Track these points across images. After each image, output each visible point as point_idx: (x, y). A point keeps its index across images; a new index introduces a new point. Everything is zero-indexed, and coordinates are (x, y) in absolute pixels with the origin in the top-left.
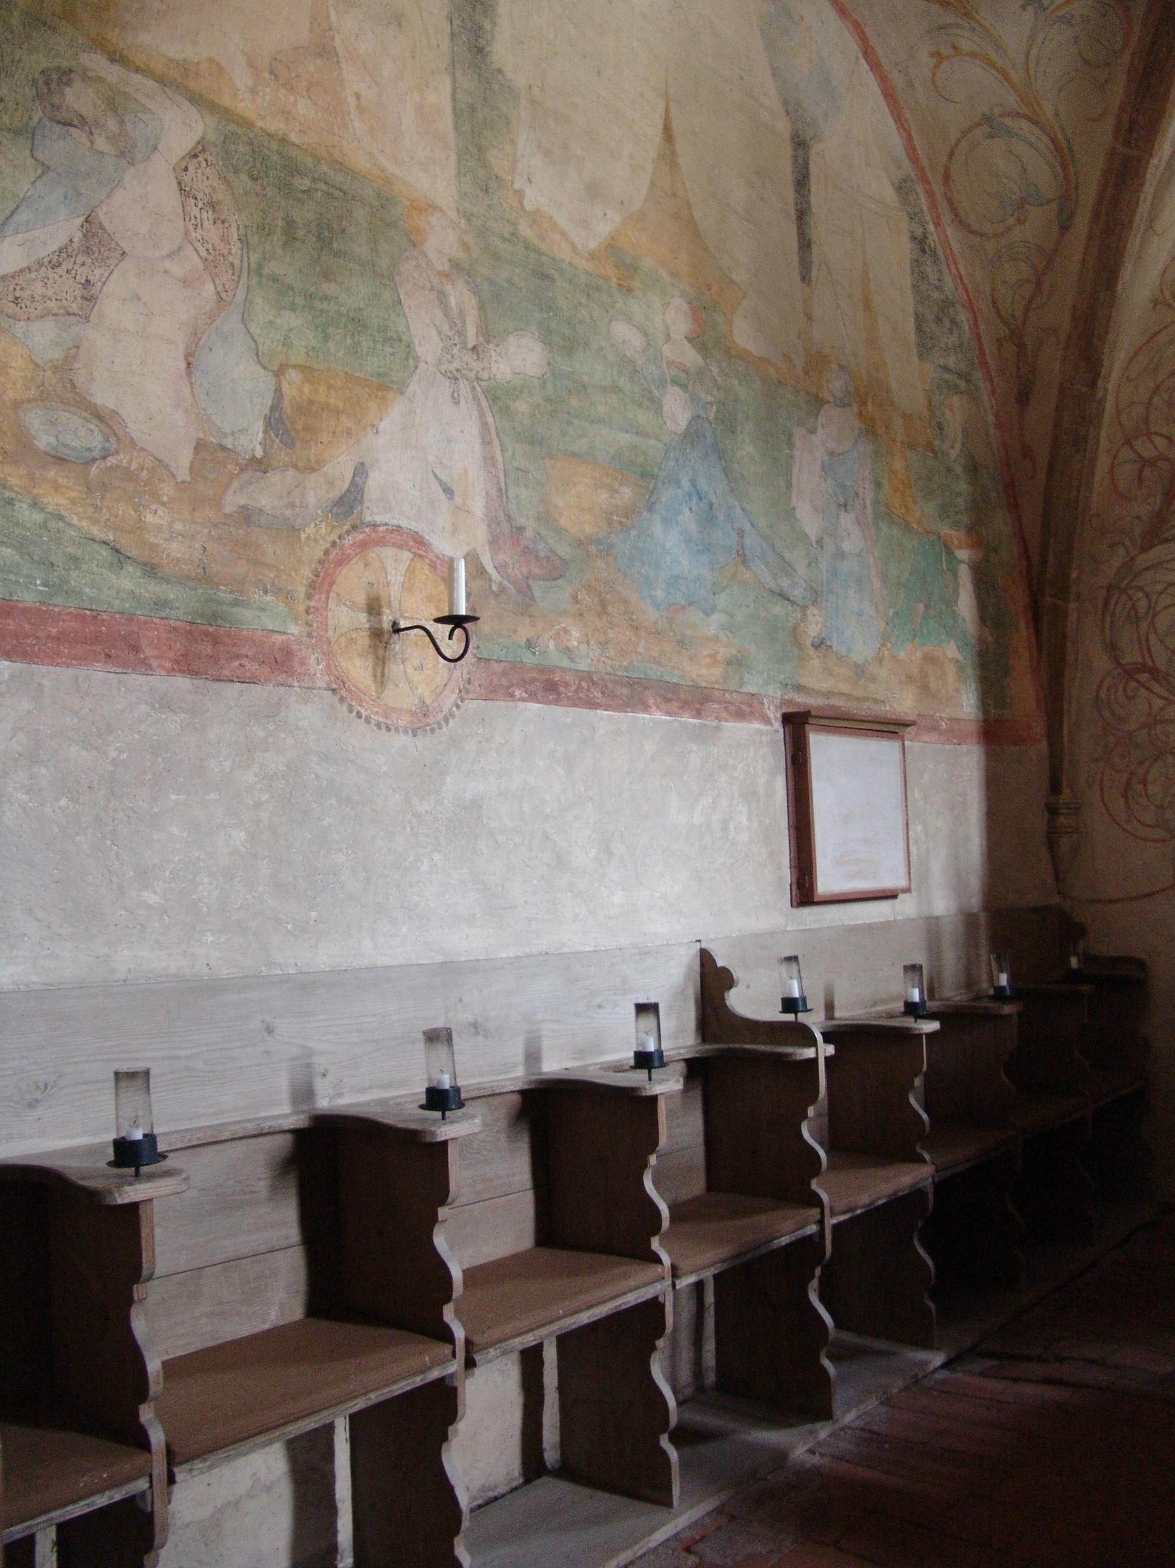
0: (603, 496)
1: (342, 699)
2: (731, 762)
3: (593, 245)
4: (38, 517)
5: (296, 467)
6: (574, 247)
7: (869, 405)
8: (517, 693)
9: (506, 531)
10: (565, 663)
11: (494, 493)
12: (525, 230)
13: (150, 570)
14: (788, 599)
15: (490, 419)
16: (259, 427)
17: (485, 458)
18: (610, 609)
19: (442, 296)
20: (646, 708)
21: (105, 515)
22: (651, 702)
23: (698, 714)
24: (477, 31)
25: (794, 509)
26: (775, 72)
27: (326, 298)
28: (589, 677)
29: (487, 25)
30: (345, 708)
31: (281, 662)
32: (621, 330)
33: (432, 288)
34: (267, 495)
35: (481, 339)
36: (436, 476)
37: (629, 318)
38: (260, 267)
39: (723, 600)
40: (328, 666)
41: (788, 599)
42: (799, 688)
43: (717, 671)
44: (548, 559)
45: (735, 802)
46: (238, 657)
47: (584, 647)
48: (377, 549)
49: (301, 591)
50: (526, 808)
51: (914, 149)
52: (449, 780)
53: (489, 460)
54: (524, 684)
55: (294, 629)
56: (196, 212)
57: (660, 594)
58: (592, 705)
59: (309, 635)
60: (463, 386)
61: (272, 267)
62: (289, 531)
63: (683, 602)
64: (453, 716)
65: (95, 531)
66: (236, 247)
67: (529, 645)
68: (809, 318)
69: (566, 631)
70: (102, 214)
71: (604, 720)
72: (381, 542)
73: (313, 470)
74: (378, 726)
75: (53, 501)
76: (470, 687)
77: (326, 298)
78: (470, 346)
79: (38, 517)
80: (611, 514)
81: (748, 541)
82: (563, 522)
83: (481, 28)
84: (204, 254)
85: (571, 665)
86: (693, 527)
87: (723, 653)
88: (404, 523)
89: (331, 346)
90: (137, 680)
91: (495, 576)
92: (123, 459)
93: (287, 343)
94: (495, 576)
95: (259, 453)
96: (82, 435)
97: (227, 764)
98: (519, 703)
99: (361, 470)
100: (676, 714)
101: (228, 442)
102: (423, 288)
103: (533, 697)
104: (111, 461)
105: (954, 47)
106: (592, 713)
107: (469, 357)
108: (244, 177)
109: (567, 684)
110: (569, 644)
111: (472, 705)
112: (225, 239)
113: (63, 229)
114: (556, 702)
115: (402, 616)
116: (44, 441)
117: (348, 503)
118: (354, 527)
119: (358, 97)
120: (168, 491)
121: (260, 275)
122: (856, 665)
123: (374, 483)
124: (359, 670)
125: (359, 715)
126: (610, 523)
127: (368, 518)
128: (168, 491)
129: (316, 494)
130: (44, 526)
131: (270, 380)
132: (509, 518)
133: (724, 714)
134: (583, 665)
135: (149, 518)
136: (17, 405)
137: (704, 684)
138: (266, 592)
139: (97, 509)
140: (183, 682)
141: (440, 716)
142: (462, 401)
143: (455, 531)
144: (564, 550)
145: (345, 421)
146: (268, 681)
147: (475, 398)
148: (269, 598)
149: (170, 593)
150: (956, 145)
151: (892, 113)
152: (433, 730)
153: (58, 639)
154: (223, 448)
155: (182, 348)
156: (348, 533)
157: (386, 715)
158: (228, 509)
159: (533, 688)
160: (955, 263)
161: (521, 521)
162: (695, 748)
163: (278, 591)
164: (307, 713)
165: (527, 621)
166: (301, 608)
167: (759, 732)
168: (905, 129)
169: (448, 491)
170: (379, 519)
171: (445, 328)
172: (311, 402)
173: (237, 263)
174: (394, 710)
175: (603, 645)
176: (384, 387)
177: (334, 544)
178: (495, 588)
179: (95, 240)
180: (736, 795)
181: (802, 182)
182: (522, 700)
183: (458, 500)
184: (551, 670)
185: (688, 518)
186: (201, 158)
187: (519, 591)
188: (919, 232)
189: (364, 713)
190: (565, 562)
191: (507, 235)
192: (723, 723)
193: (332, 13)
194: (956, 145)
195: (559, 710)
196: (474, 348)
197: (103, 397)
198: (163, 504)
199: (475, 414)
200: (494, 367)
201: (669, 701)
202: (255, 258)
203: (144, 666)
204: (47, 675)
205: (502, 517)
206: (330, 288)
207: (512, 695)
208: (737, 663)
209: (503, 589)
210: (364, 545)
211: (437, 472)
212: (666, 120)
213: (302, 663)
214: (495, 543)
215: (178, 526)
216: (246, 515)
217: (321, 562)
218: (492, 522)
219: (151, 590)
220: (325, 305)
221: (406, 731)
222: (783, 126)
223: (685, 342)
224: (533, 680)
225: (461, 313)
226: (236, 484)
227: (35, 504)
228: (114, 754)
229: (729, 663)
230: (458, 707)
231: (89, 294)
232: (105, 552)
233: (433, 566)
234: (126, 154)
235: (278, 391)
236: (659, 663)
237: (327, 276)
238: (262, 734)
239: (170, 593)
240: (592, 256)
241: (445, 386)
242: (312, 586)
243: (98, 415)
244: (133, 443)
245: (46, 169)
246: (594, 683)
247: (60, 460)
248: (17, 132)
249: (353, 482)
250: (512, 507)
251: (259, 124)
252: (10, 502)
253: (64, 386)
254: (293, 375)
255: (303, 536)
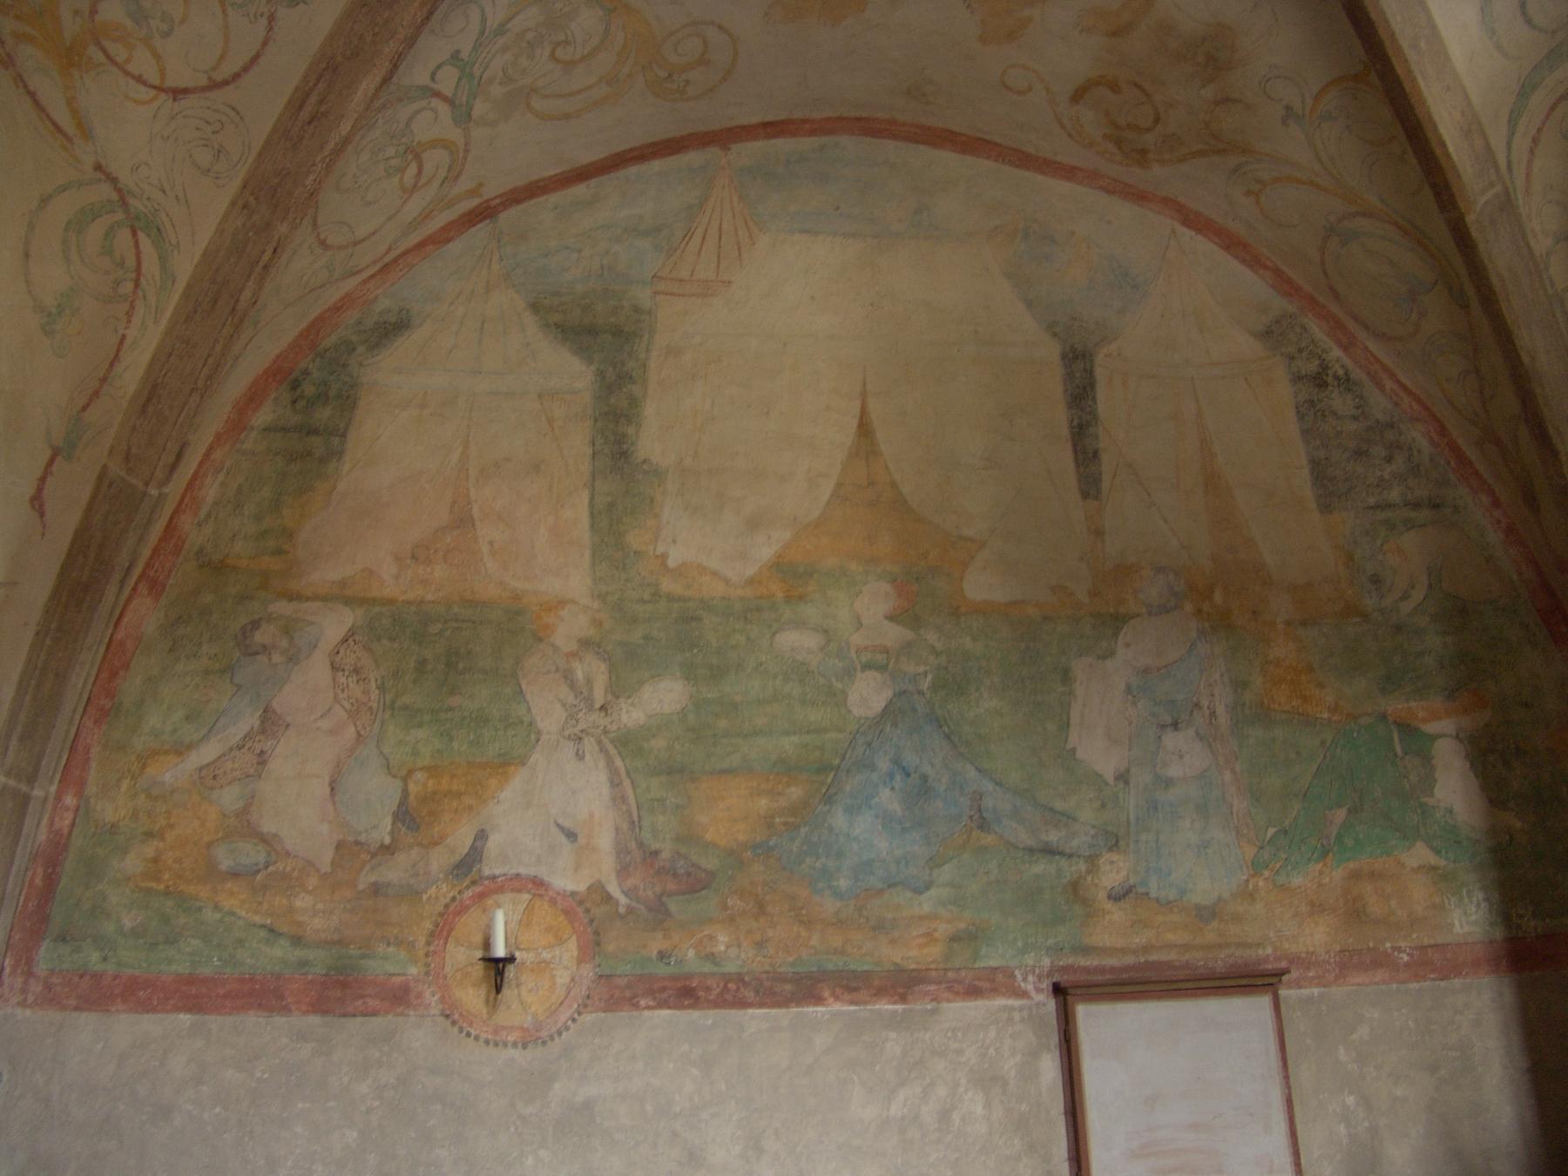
0: (763, 803)
1: (454, 1023)
2: (954, 1045)
3: (750, 571)
4: (218, 916)
5: (420, 844)
6: (727, 581)
7: (1219, 600)
8: (643, 1003)
9: (637, 855)
10: (708, 968)
11: (625, 826)
12: (667, 585)
13: (297, 941)
14: (1061, 854)
15: (619, 762)
16: (389, 820)
17: (614, 799)
18: (769, 908)
19: (568, 677)
20: (819, 1000)
21: (265, 906)
22: (826, 994)
23: (903, 999)
24: (621, 439)
25: (1074, 750)
26: (1029, 304)
27: (451, 709)
28: (739, 979)
29: (631, 430)
30: (456, 1029)
31: (400, 997)
32: (789, 639)
33: (557, 670)
34: (394, 872)
35: (610, 697)
36: (558, 825)
37: (799, 624)
38: (393, 702)
39: (946, 873)
40: (443, 997)
41: (1061, 854)
42: (1087, 950)
43: (935, 951)
44: (689, 874)
45: (961, 1090)
46: (363, 996)
47: (733, 952)
48: (495, 897)
49: (422, 940)
50: (649, 1108)
51: (1290, 281)
52: (557, 1086)
53: (618, 799)
54: (651, 992)
55: (413, 970)
56: (343, 680)
57: (843, 883)
58: (743, 1004)
59: (427, 974)
60: (589, 744)
61: (406, 699)
62: (412, 894)
63: (879, 885)
64: (567, 1029)
65: (257, 919)
66: (374, 694)
67: (662, 956)
68: (1099, 533)
69: (711, 938)
70: (275, 705)
71: (756, 1019)
72: (500, 890)
73: (436, 844)
74: (487, 1042)
75: (228, 903)
76: (589, 1002)
77: (451, 709)
78: (597, 706)
79: (218, 916)
80: (773, 817)
81: (988, 803)
82: (709, 837)
83: (624, 436)
84: (348, 706)
85: (716, 969)
86: (896, 807)
87: (943, 929)
88: (523, 871)
89: (455, 745)
90: (280, 1020)
91: (623, 900)
92: (280, 866)
93: (415, 753)
94: (623, 900)
95: (387, 840)
96: (251, 854)
97: (346, 1079)
98: (646, 1013)
99: (482, 836)
100: (865, 1003)
101: (363, 838)
102: (548, 672)
103: (662, 1005)
104: (271, 869)
105: (1259, 181)
106: (741, 1012)
107: (596, 717)
108: (385, 642)
109: (708, 989)
110: (715, 950)
111: (588, 1018)
112: (366, 692)
113: (250, 720)
114: (692, 1007)
115: (518, 948)
116: (226, 864)
117: (467, 865)
118: (474, 883)
119: (491, 543)
120: (312, 882)
121: (392, 708)
122: (1199, 909)
123: (493, 844)
124: (472, 997)
125: (469, 1035)
126: (770, 826)
127: (487, 872)
128: (312, 882)
129: (439, 860)
130: (221, 921)
131: (398, 783)
132: (641, 845)
133: (946, 995)
134: (731, 968)
135: (298, 903)
136: (209, 845)
137: (913, 966)
138: (389, 944)
139: (260, 903)
140: (315, 1020)
141: (554, 1029)
142: (588, 757)
143: (577, 867)
144: (710, 863)
145: (468, 800)
146: (387, 1013)
147: (603, 750)
148: (391, 949)
149: (310, 954)
150: (1323, 262)
151: (1243, 261)
152: (544, 1043)
153: (225, 996)
154: (357, 843)
155: (327, 780)
156: (468, 887)
157: (496, 1032)
158: (361, 887)
159: (664, 995)
160: (1392, 376)
161: (655, 846)
162: (893, 1035)
163: (399, 943)
164: (418, 1035)
165: (659, 935)
166: (421, 953)
167: (1011, 1009)
168: (1266, 267)
169: (571, 835)
170: (497, 872)
171: (571, 699)
172: (435, 793)
173: (375, 705)
174: (504, 1028)
175: (760, 945)
176: (505, 765)
177: (454, 899)
178: (622, 910)
179: (270, 723)
180: (963, 1081)
181: (1081, 394)
182: (648, 1008)
183: (582, 840)
184: (689, 976)
185: (888, 799)
186: (351, 641)
187: (650, 910)
188: (1313, 366)
189: (473, 1032)
190: (712, 875)
191: (646, 596)
192: (945, 1005)
193: (472, 492)
194: (1323, 262)
195: (695, 1015)
196: (602, 708)
197: (268, 826)
198: (309, 892)
199: (602, 764)
200: (624, 717)
201: (856, 990)
202: (389, 697)
203: (285, 1010)
204: (214, 1022)
205: (633, 845)
206: (455, 701)
207: (636, 1006)
208: (970, 938)
209: (630, 910)
210: (482, 896)
211: (560, 821)
212: (861, 418)
213: (419, 996)
214: (623, 871)
215: (320, 906)
216: (376, 890)
217: (441, 915)
218: (621, 851)
219: (299, 953)
220: (450, 715)
221: (515, 1045)
222: (1051, 351)
223: (886, 622)
224: (664, 989)
225: (589, 682)
226: (367, 867)
227: (217, 908)
228: (258, 1075)
229: (954, 939)
230: (574, 1020)
231: (262, 759)
232: (263, 933)
233: (553, 902)
234: (293, 659)
235: (405, 793)
236: (843, 952)
237: (452, 693)
238: (377, 1055)
239: (310, 954)
240: (751, 582)
241: (569, 748)
242: (432, 934)
243: (265, 840)
244: (288, 854)
245: (239, 687)
246: (745, 983)
247: (235, 875)
248: (222, 671)
249: (473, 848)
250: (646, 835)
251: (405, 598)
252: (200, 909)
253: (244, 826)
254: (420, 776)
255: (425, 897)
